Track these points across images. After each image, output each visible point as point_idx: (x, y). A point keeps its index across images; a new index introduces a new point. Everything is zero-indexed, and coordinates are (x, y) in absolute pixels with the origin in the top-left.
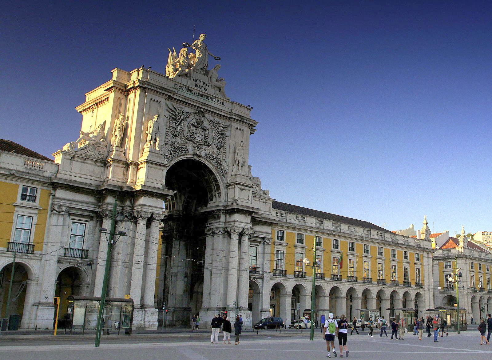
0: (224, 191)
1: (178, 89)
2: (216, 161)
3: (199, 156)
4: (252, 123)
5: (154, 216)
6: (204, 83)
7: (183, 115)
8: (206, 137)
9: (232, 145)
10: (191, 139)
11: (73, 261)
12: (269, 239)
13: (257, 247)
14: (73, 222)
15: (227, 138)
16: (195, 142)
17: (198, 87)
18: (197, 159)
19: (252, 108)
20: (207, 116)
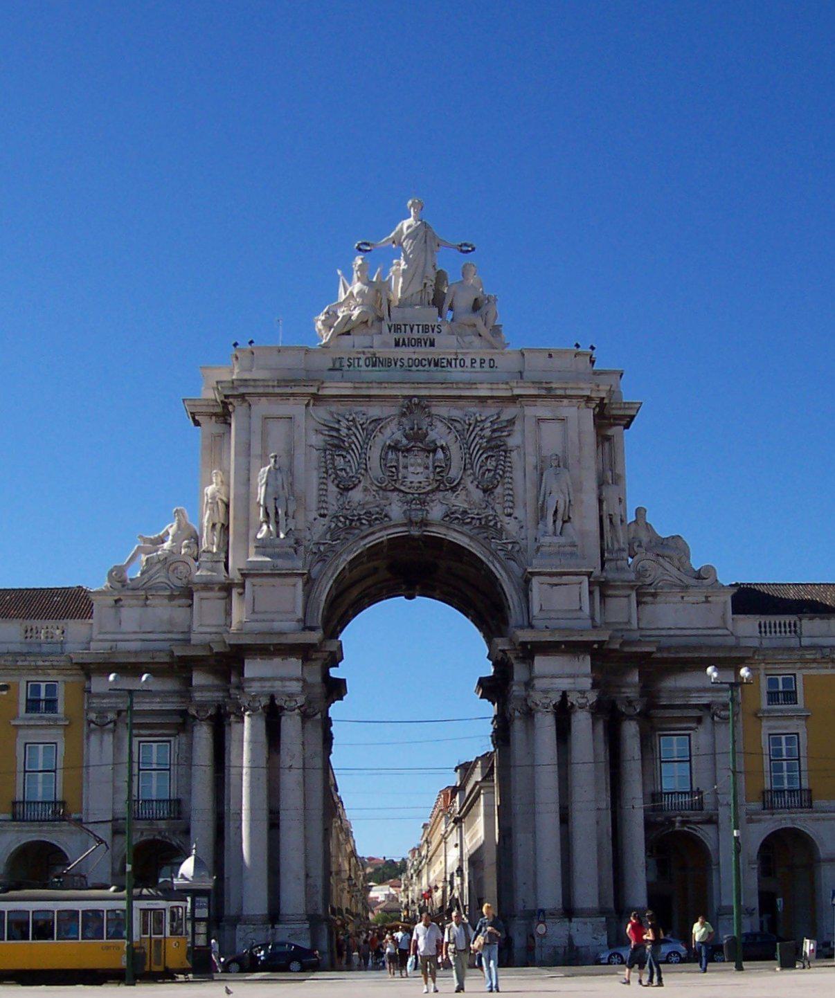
0: (515, 597)
1: (346, 368)
2: (481, 523)
3: (424, 523)
4: (587, 393)
5: (276, 702)
6: (426, 329)
7: (363, 429)
8: (441, 470)
9: (529, 469)
10: (391, 483)
11: (148, 827)
12: (725, 706)
13: (689, 735)
14: (140, 742)
15: (514, 454)
16: (408, 491)
17: (404, 344)
18: (415, 532)
19: (592, 348)
20: (442, 410)
